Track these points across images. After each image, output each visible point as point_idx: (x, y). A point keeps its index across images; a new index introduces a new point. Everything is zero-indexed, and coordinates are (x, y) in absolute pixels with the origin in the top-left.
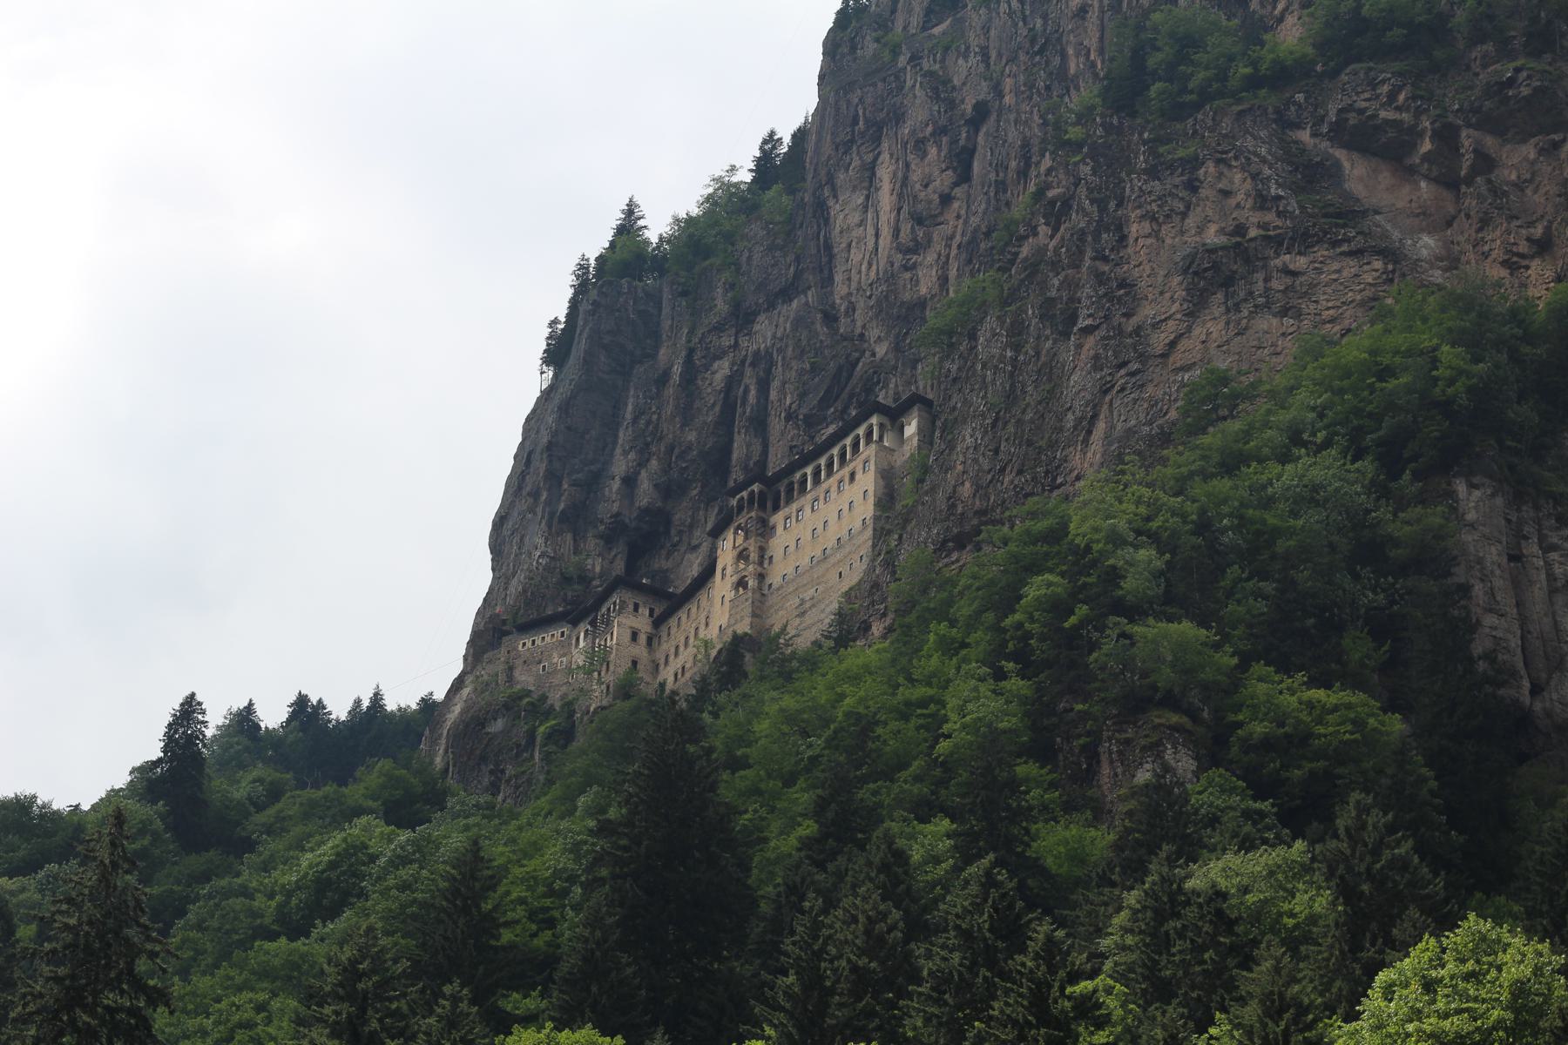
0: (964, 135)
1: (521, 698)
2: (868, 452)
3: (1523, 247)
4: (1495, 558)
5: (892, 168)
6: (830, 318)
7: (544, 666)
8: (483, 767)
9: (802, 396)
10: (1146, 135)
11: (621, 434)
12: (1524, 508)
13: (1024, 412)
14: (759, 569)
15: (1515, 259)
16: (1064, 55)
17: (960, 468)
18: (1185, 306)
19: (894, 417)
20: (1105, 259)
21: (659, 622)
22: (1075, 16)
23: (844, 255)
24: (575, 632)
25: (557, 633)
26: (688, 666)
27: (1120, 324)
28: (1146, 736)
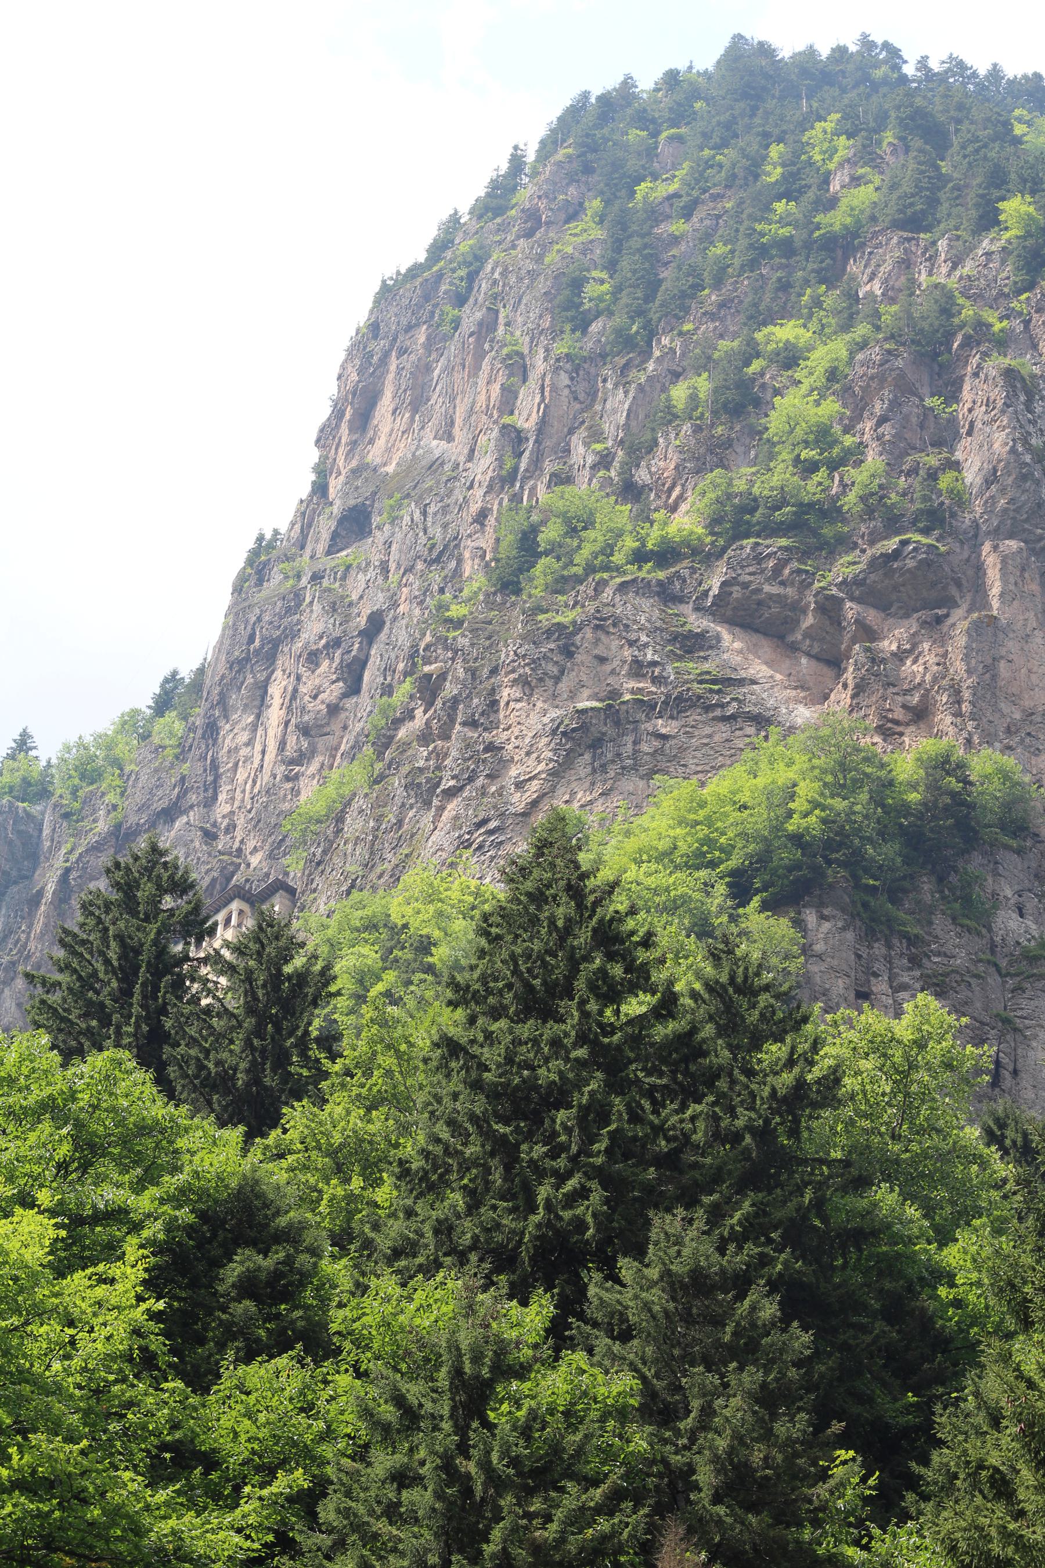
0: (357, 646)
3: (899, 714)
4: (841, 992)
5: (284, 683)
12: (876, 945)
13: (380, 877)
15: (889, 725)
16: (460, 561)
18: (551, 766)
22: (475, 521)
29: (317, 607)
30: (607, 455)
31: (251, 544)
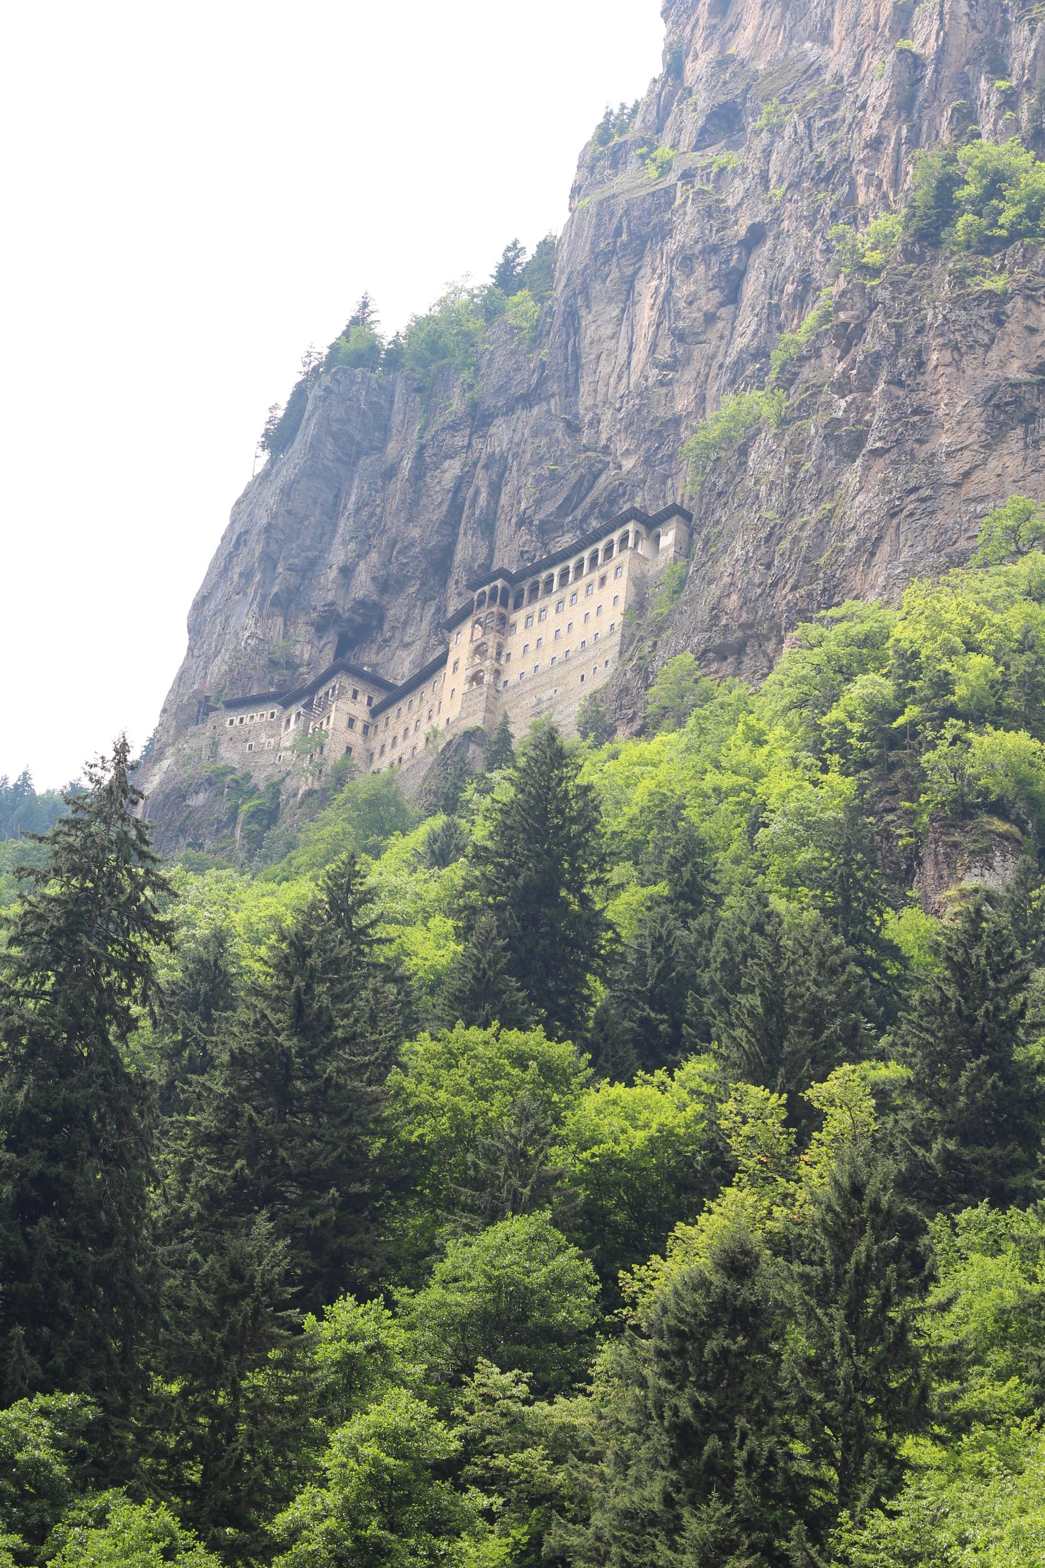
1: (224, 774)
2: (621, 558)
6: (573, 428)
7: (251, 746)
8: (181, 839)
9: (539, 503)
10: (951, 265)
11: (342, 523)
13: (801, 528)
14: (496, 665)
16: (853, 184)
17: (727, 580)
18: (983, 438)
19: (652, 525)
20: (901, 384)
21: (375, 713)
22: (866, 146)
23: (592, 366)
24: (288, 712)
25: (267, 714)
26: (405, 757)
27: (912, 450)
28: (975, 841)
29: (690, 209)
30: (1012, 95)
31: (600, 120)
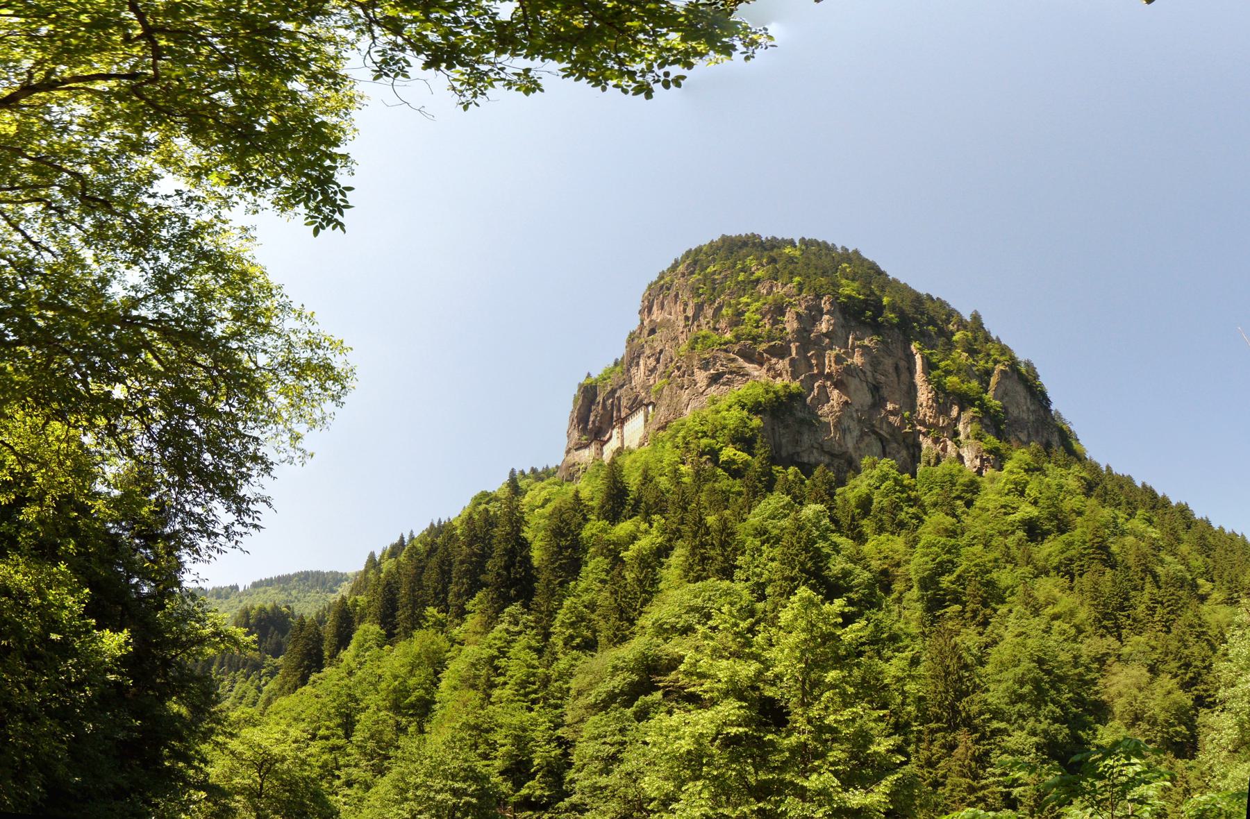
19: (647, 405)
